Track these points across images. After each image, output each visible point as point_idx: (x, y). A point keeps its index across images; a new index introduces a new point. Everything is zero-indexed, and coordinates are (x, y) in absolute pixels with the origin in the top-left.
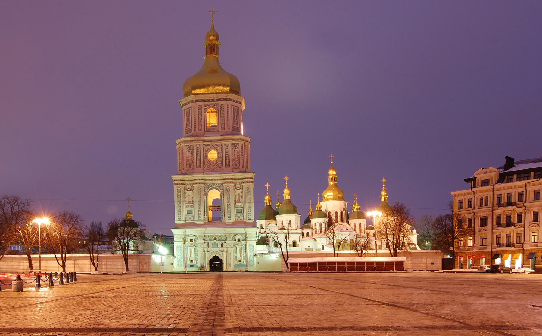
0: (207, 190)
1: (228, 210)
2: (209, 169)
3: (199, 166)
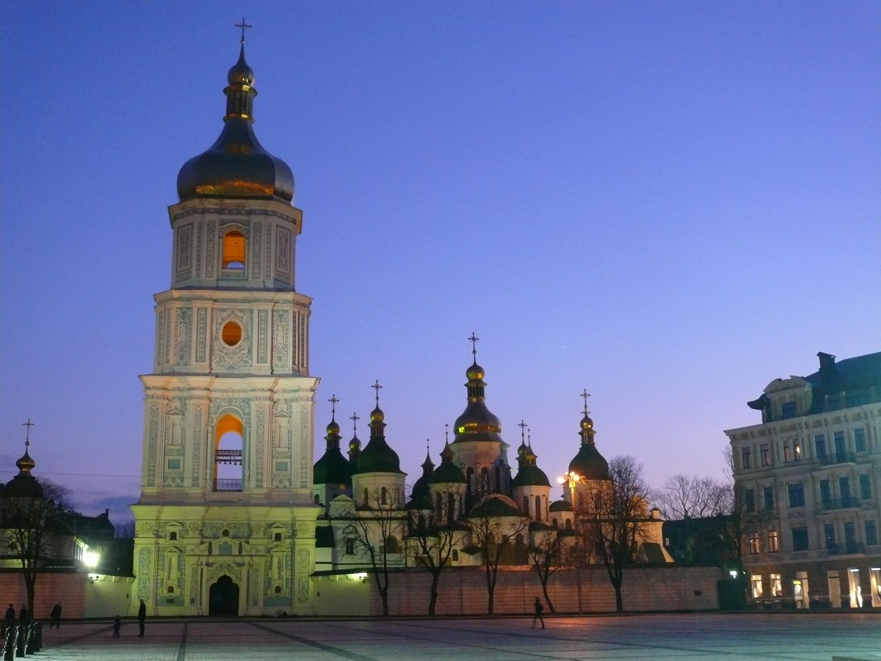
0: (216, 414)
1: (257, 464)
2: (222, 363)
3: (201, 358)
